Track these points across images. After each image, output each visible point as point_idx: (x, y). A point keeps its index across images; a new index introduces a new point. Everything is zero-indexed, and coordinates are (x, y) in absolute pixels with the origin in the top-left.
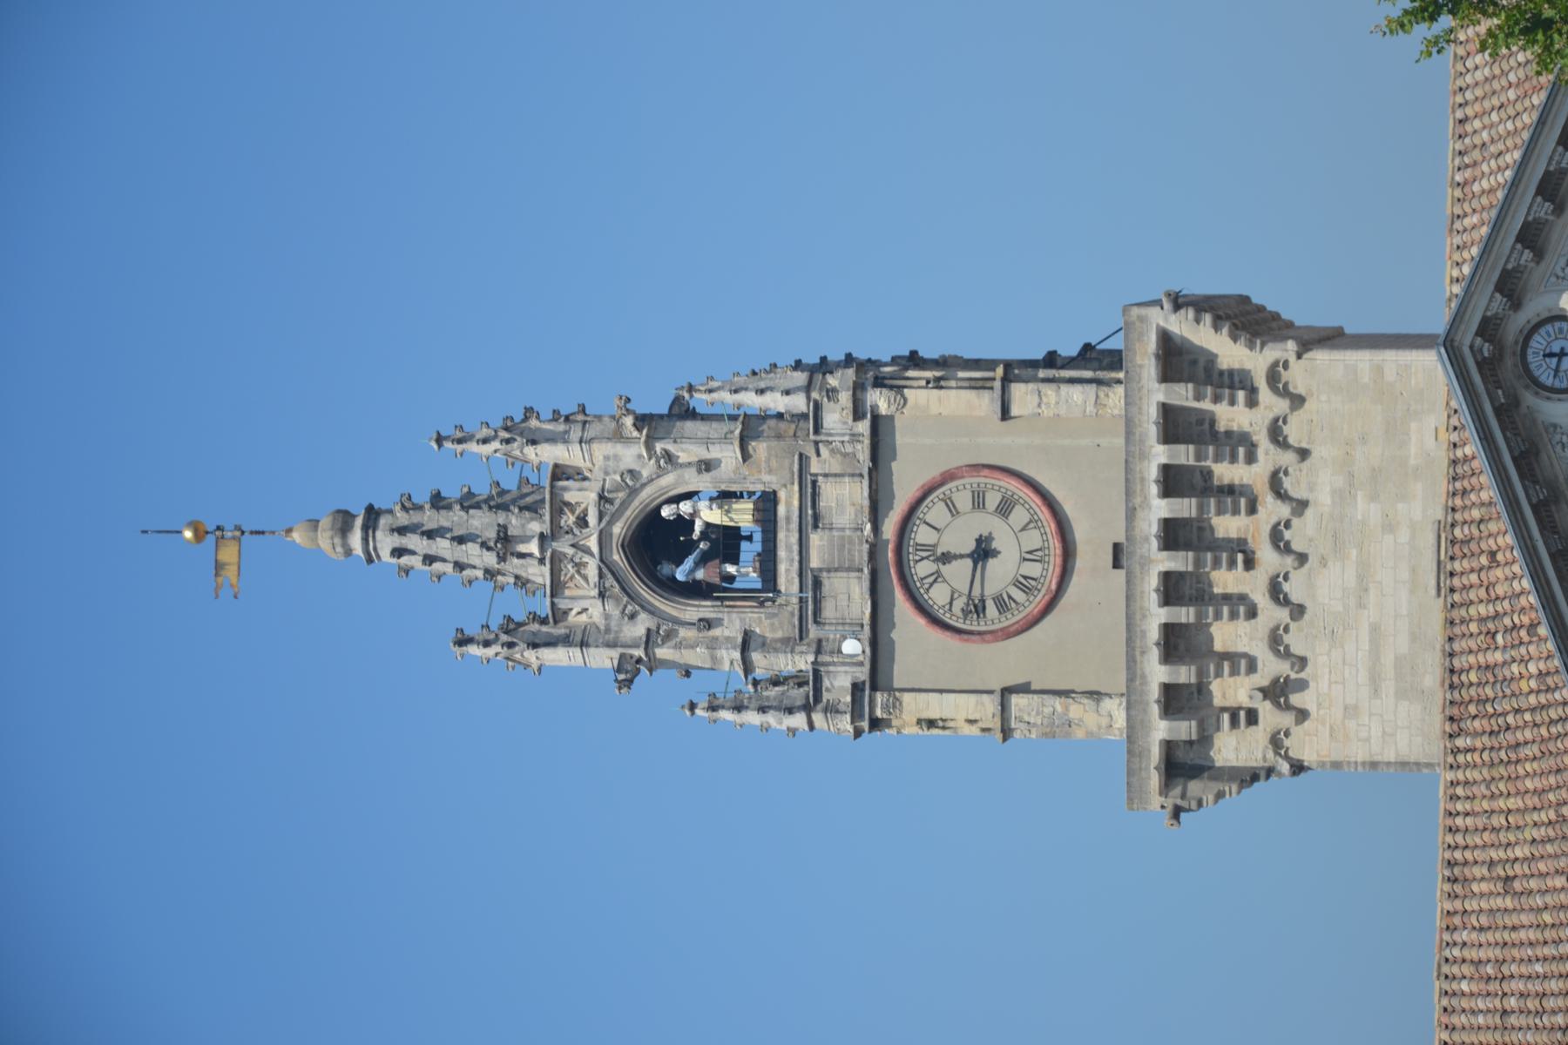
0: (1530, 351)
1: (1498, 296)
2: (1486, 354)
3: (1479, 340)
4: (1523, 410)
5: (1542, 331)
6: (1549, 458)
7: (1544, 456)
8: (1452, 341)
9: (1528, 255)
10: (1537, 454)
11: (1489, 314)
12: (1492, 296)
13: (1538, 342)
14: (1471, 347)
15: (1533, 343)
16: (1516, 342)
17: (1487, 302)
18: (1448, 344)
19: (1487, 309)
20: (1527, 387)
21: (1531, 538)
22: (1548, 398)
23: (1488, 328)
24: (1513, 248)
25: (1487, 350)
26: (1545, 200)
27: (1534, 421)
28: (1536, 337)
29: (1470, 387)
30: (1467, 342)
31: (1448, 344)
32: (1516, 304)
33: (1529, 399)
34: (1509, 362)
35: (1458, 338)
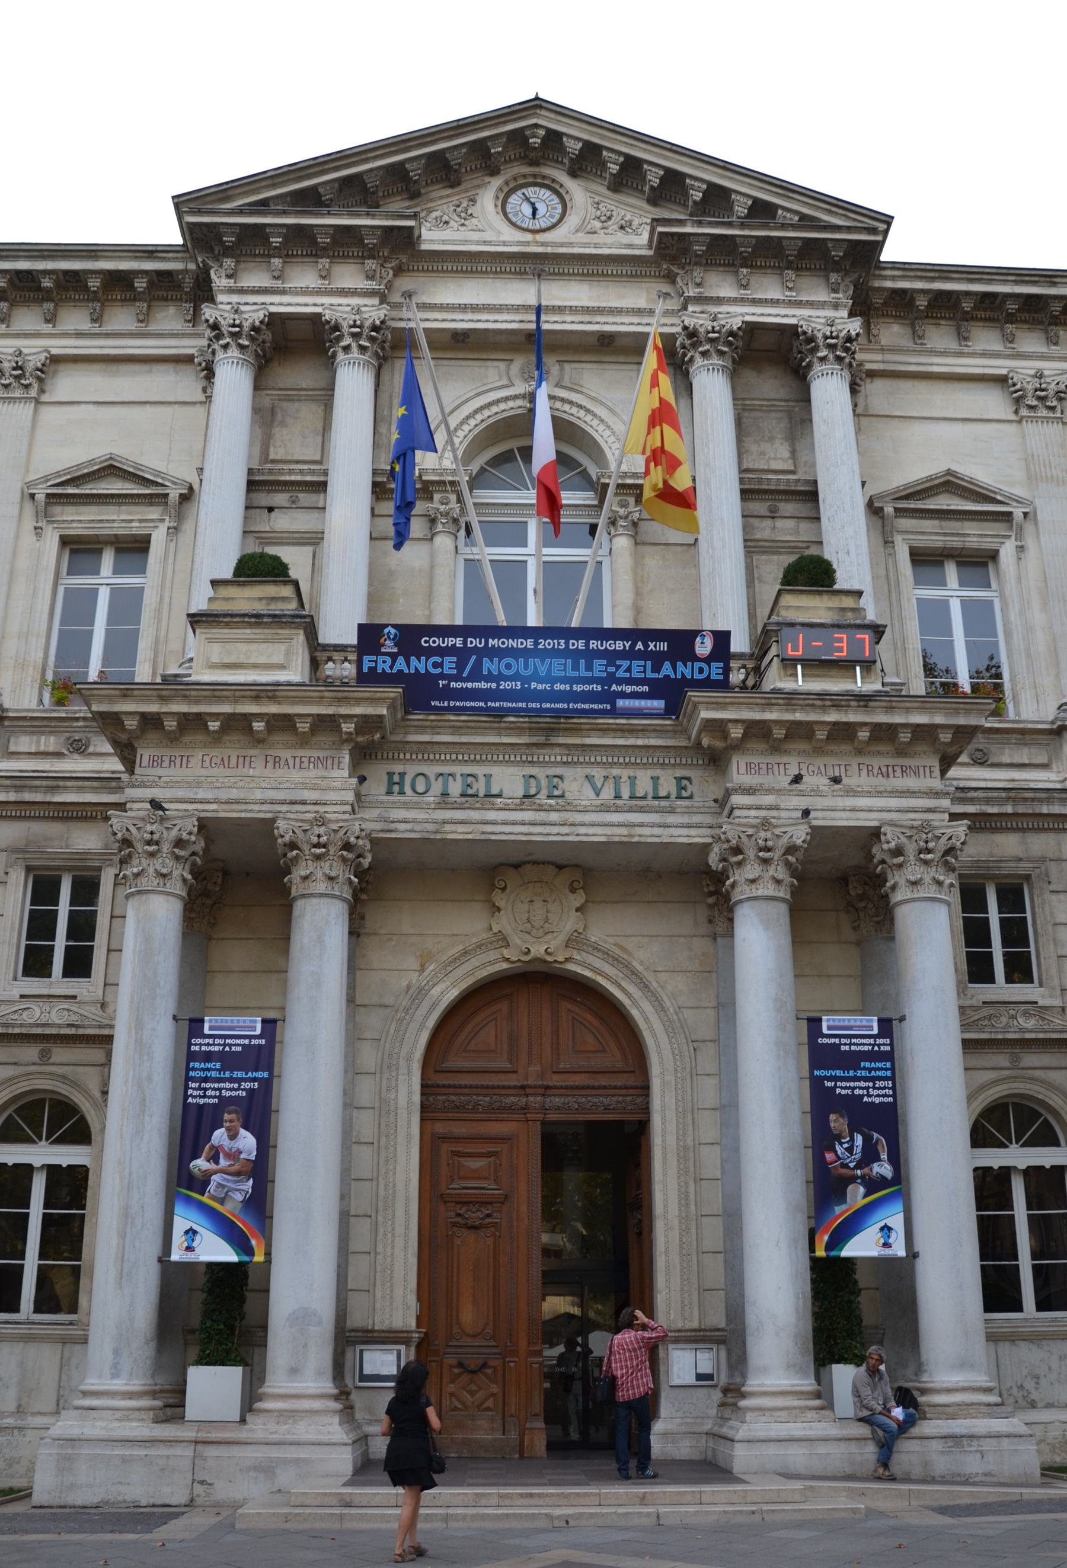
0: (537, 189)
1: (580, 144)
2: (531, 141)
3: (542, 132)
4: (487, 179)
5: (554, 197)
6: (448, 196)
7: (449, 191)
8: (540, 107)
9: (614, 168)
10: (452, 187)
11: (565, 139)
12: (579, 139)
13: (544, 193)
14: (536, 126)
15: (543, 191)
16: (544, 177)
17: (575, 135)
18: (537, 102)
19: (569, 136)
20: (507, 183)
21: (375, 158)
22: (497, 197)
23: (554, 138)
24: (620, 153)
25: (535, 141)
26: (662, 179)
27: (479, 187)
28: (548, 193)
29: (502, 120)
30: (540, 122)
31: (537, 102)
32: (573, 174)
33: (496, 182)
34: (527, 170)
35: (543, 112)
